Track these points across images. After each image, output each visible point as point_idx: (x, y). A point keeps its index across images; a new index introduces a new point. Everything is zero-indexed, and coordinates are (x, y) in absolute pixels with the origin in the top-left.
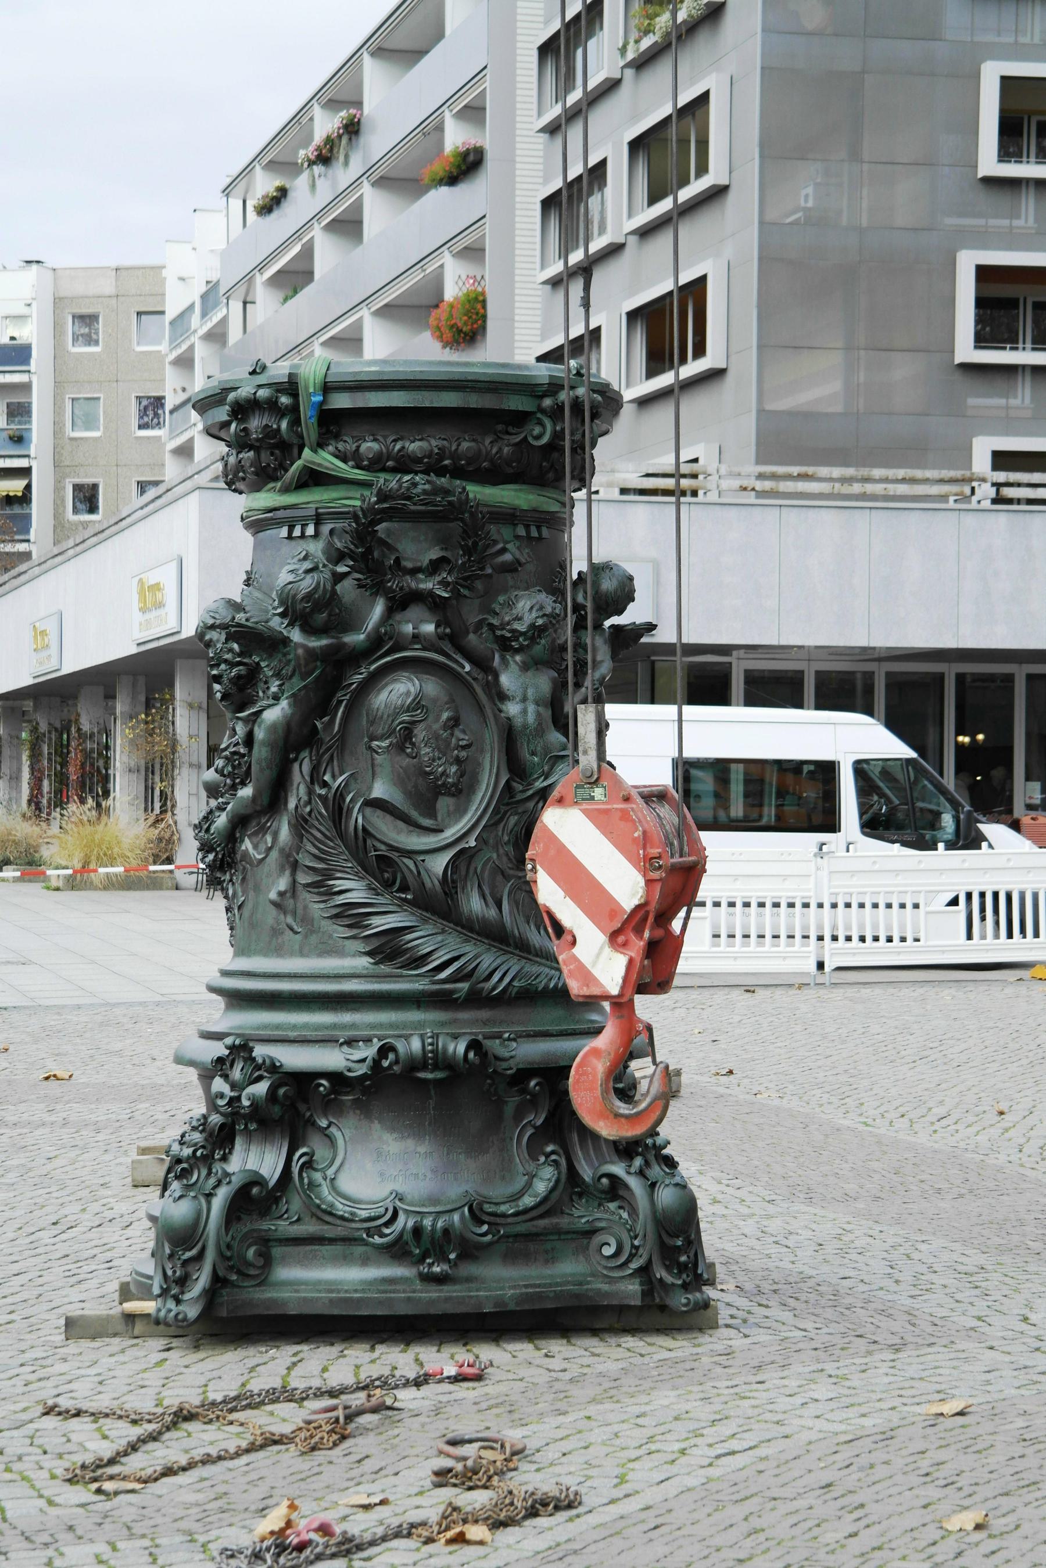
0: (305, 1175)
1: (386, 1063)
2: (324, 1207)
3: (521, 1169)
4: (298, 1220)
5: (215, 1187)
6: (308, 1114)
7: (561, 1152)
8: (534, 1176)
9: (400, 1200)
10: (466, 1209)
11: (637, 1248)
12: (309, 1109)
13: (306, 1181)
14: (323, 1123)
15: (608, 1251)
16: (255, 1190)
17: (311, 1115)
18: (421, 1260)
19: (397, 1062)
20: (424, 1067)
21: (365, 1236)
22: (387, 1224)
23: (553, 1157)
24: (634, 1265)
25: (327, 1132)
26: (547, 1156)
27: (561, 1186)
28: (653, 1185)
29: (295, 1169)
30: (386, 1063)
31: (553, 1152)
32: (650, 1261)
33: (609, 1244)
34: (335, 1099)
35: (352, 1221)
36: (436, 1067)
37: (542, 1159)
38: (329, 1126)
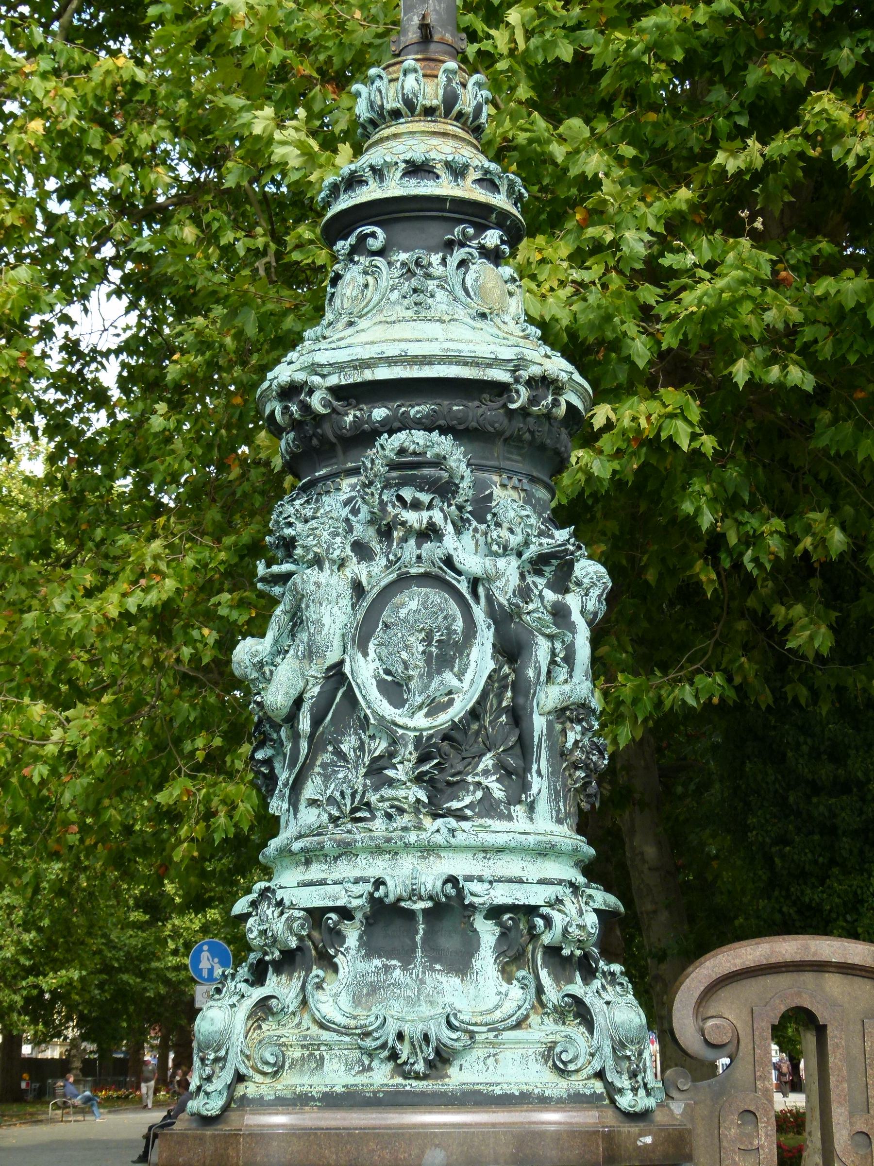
16: (274, 1002)
29: (309, 988)
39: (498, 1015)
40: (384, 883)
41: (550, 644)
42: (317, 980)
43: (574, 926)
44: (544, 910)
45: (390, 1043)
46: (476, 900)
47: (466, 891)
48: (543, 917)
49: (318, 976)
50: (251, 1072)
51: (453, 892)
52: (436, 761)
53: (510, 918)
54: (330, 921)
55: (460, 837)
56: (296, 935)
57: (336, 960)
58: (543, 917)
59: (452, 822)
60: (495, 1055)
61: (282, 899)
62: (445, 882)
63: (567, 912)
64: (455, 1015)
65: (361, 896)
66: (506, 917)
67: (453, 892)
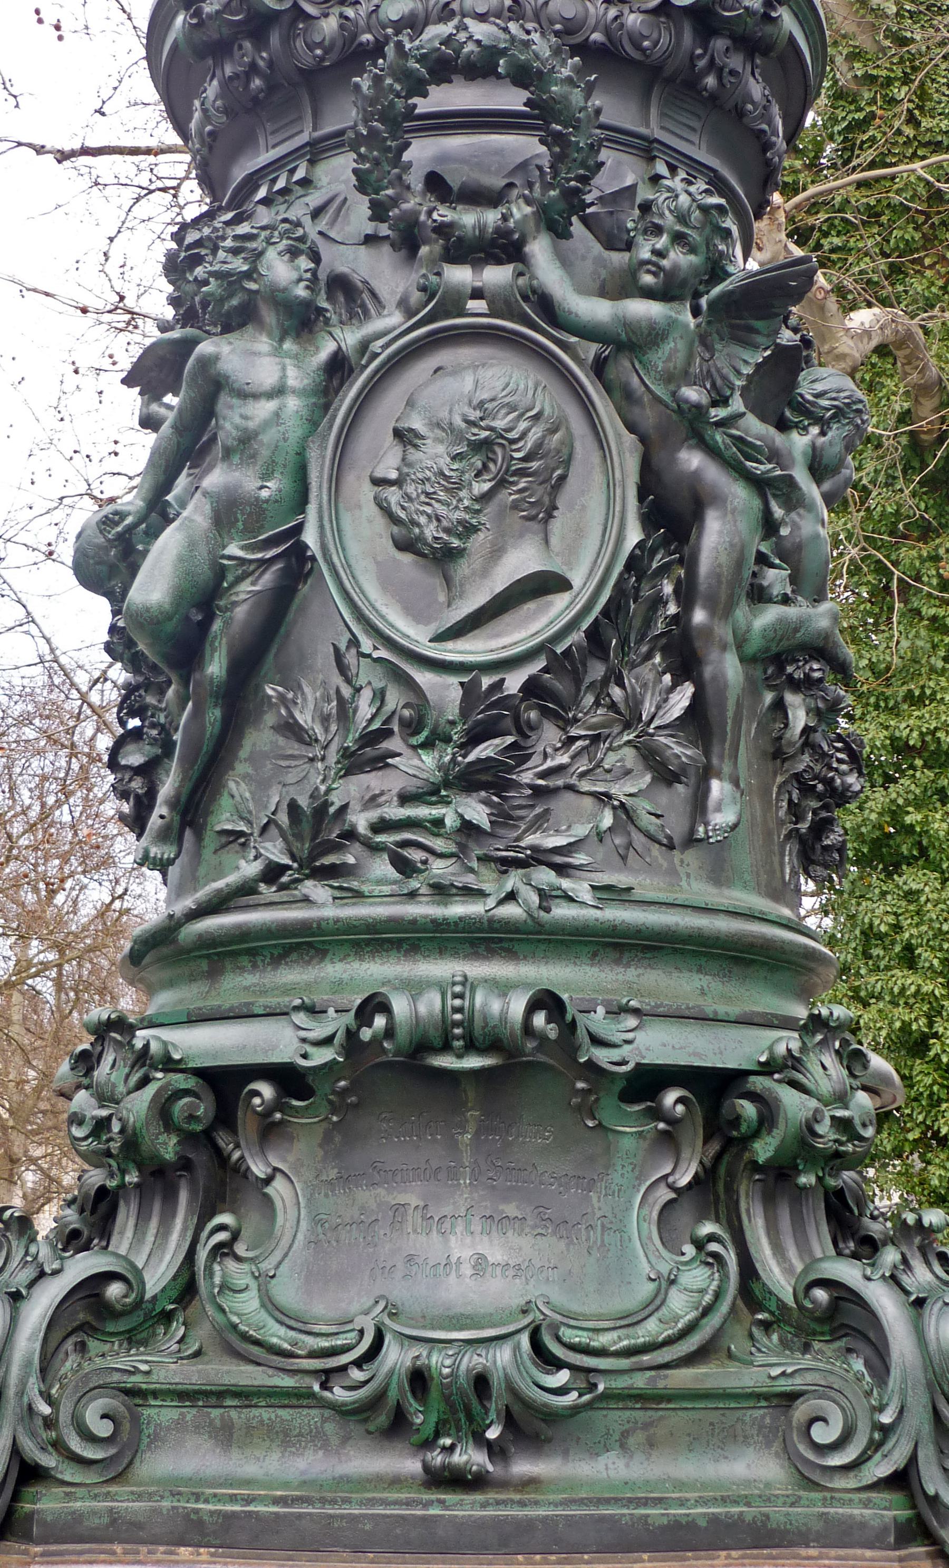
0: (217, 1267)
1: (366, 1034)
2: (243, 1328)
3: (645, 1268)
4: (198, 1354)
5: (31, 1285)
6: (236, 1155)
7: (725, 1236)
8: (672, 1282)
9: (391, 1315)
10: (525, 1340)
11: (886, 1430)
12: (237, 1146)
13: (217, 1280)
14: (258, 1169)
15: (822, 1434)
16: (114, 1290)
17: (242, 1158)
18: (428, 1444)
19: (389, 1032)
20: (446, 1047)
21: (316, 1388)
22: (358, 1363)
23: (714, 1247)
24: (880, 1469)
25: (269, 1190)
26: (699, 1245)
27: (724, 1308)
28: (919, 1303)
29: (202, 1255)
30: (366, 1034)
31: (712, 1238)
32: (913, 1459)
33: (825, 1420)
34: (282, 1122)
35: (291, 1355)
36: (472, 1046)
37: (689, 1250)
38: (268, 1181)
39: (651, 1329)
40: (385, 1008)
41: (757, 503)
42: (222, 1236)
43: (827, 1121)
44: (759, 1083)
45: (393, 1394)
46: (603, 1056)
47: (581, 1033)
48: (753, 1097)
49: (222, 1228)
50: (48, 1460)
51: (552, 1031)
52: (510, 740)
53: (679, 1100)
54: (257, 1101)
55: (562, 912)
56: (179, 1130)
57: (269, 1190)
58: (753, 1097)
59: (545, 876)
60: (646, 1426)
61: (147, 1046)
62: (533, 1007)
63: (810, 1085)
64: (554, 1329)
65: (327, 1041)
66: (670, 1097)
67: (552, 1031)
